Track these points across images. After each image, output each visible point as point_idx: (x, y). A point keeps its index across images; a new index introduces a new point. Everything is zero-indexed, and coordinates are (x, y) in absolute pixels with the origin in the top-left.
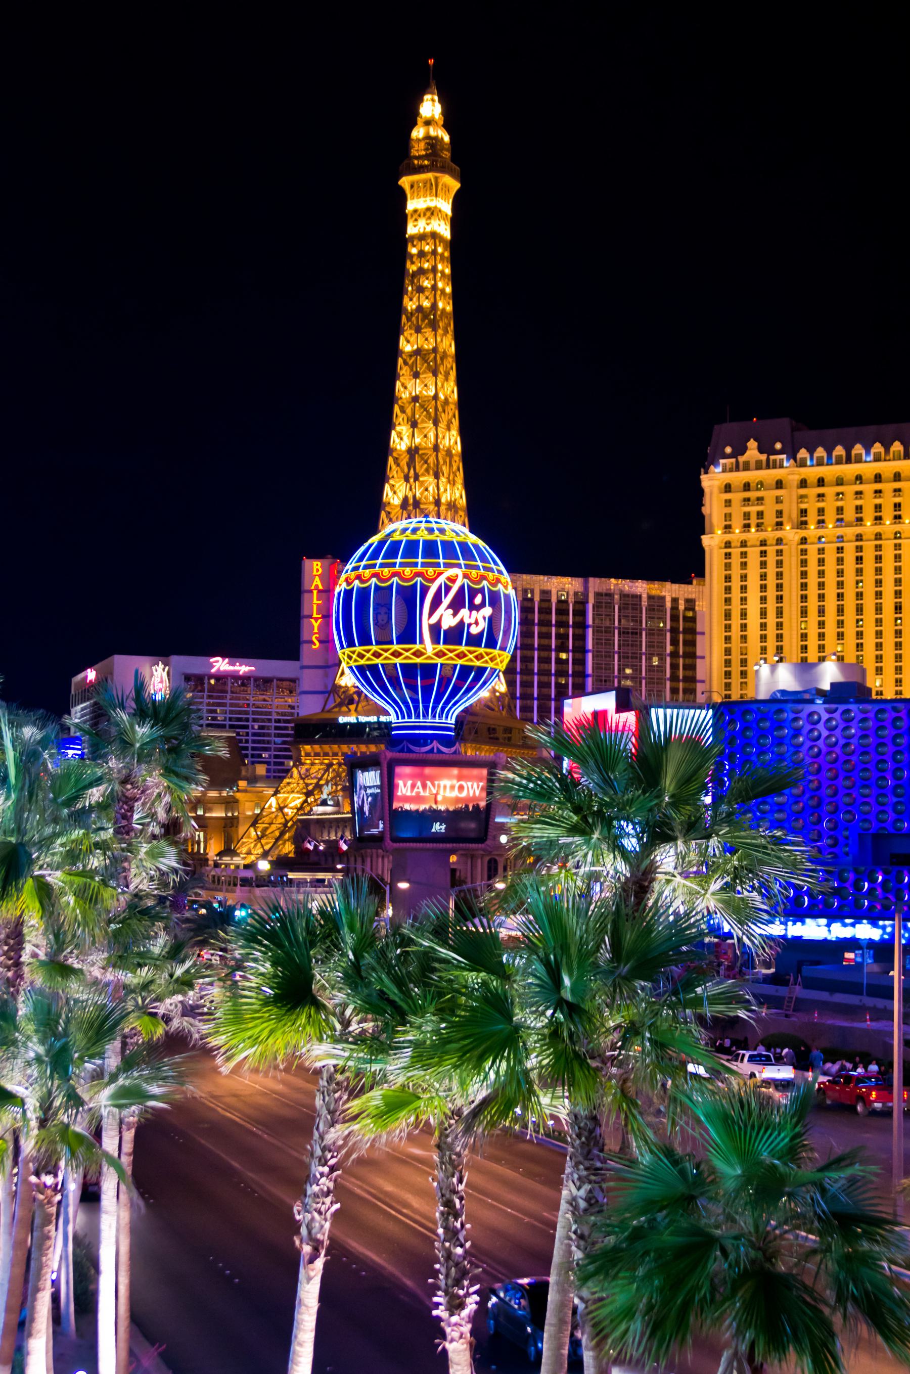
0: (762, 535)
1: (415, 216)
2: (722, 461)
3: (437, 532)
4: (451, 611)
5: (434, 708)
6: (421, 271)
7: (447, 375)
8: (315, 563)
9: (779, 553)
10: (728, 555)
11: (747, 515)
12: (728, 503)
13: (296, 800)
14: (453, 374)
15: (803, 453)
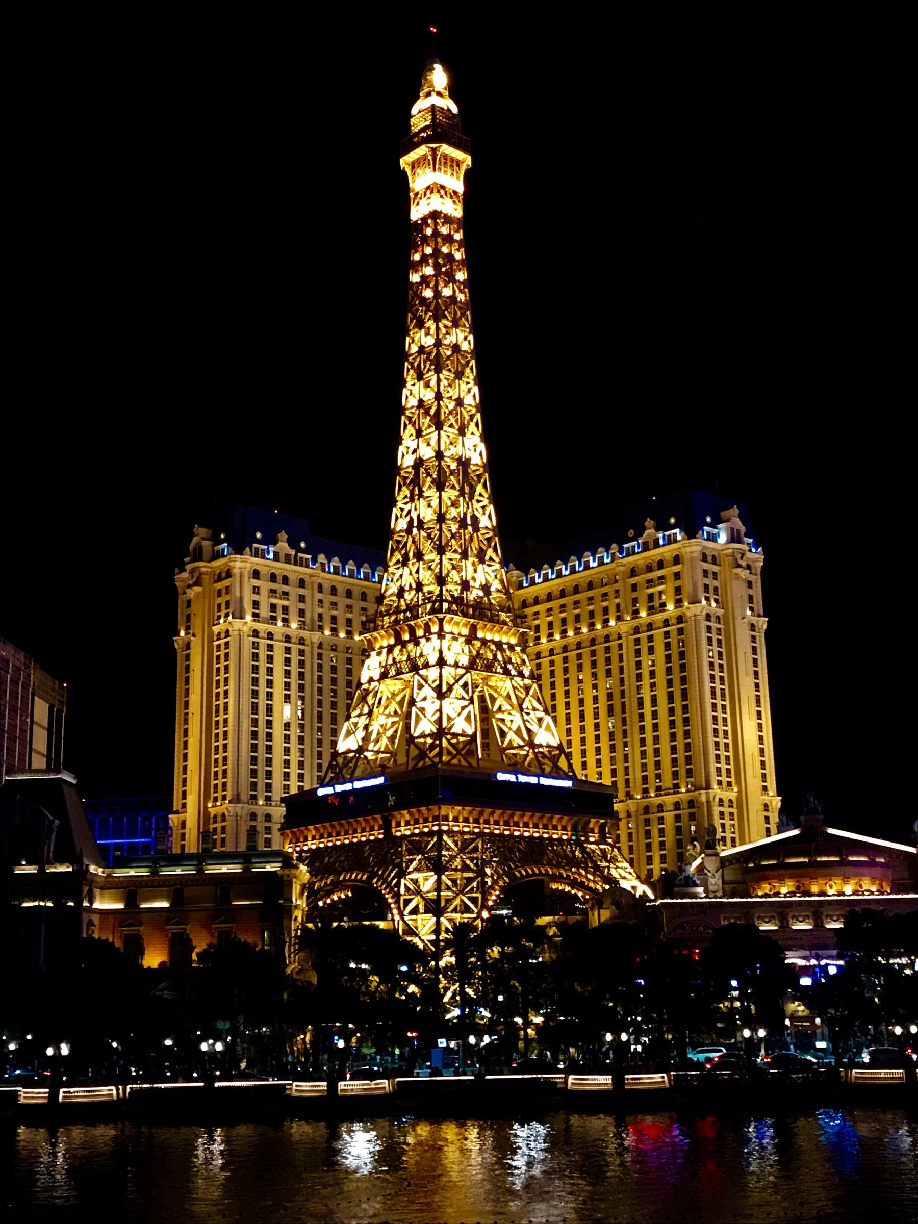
1: (442, 192)
9: (302, 653)
10: (255, 645)
11: (273, 607)
12: (256, 590)
15: (322, 558)
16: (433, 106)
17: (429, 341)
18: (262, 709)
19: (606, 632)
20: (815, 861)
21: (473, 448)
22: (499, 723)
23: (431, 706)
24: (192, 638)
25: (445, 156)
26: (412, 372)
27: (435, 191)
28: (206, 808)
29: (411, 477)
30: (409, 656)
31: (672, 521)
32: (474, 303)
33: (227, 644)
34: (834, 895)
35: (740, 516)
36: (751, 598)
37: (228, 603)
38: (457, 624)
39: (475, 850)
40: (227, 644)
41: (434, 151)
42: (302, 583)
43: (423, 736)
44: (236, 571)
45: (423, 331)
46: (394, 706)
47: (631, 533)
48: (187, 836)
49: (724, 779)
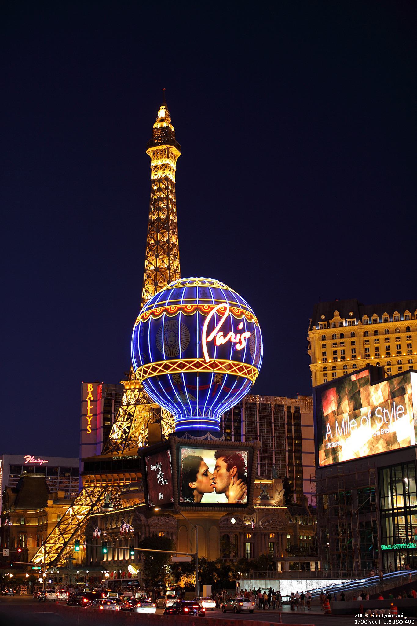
0: (344, 363)
3: (207, 283)
4: (221, 333)
5: (207, 409)
6: (160, 199)
7: (175, 258)
8: (89, 385)
11: (335, 352)
12: (324, 346)
13: (85, 509)
14: (178, 256)
15: (365, 317)
25: (158, 151)
42: (353, 335)
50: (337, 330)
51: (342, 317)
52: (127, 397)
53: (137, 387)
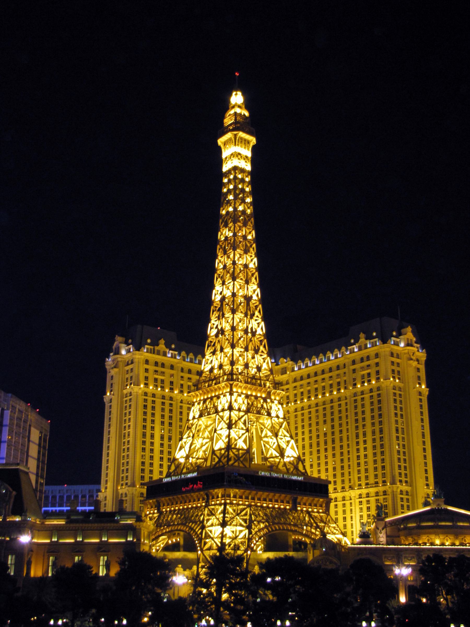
0: (163, 393)
1: (239, 157)
2: (146, 346)
9: (171, 405)
10: (146, 400)
11: (156, 380)
12: (147, 370)
15: (183, 353)
16: (235, 113)
17: (231, 234)
18: (148, 435)
19: (339, 395)
20: (438, 525)
21: (254, 290)
22: (265, 443)
23: (225, 432)
24: (113, 397)
26: (221, 250)
27: (235, 156)
28: (117, 489)
29: (219, 306)
30: (214, 405)
31: (374, 334)
32: (256, 214)
33: (130, 399)
34: (449, 545)
35: (413, 332)
36: (419, 378)
37: (131, 377)
38: (240, 387)
39: (246, 515)
40: (130, 399)
41: (235, 135)
43: (220, 449)
44: (136, 360)
45: (227, 229)
46: (207, 434)
47: (352, 341)
48: (107, 505)
49: (403, 479)
50: (159, 358)
51: (167, 347)
52: (235, 401)
53: (244, 392)
